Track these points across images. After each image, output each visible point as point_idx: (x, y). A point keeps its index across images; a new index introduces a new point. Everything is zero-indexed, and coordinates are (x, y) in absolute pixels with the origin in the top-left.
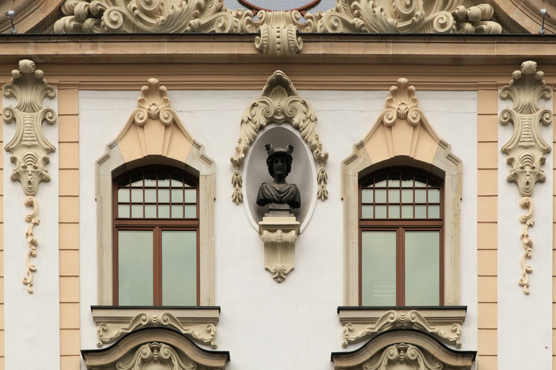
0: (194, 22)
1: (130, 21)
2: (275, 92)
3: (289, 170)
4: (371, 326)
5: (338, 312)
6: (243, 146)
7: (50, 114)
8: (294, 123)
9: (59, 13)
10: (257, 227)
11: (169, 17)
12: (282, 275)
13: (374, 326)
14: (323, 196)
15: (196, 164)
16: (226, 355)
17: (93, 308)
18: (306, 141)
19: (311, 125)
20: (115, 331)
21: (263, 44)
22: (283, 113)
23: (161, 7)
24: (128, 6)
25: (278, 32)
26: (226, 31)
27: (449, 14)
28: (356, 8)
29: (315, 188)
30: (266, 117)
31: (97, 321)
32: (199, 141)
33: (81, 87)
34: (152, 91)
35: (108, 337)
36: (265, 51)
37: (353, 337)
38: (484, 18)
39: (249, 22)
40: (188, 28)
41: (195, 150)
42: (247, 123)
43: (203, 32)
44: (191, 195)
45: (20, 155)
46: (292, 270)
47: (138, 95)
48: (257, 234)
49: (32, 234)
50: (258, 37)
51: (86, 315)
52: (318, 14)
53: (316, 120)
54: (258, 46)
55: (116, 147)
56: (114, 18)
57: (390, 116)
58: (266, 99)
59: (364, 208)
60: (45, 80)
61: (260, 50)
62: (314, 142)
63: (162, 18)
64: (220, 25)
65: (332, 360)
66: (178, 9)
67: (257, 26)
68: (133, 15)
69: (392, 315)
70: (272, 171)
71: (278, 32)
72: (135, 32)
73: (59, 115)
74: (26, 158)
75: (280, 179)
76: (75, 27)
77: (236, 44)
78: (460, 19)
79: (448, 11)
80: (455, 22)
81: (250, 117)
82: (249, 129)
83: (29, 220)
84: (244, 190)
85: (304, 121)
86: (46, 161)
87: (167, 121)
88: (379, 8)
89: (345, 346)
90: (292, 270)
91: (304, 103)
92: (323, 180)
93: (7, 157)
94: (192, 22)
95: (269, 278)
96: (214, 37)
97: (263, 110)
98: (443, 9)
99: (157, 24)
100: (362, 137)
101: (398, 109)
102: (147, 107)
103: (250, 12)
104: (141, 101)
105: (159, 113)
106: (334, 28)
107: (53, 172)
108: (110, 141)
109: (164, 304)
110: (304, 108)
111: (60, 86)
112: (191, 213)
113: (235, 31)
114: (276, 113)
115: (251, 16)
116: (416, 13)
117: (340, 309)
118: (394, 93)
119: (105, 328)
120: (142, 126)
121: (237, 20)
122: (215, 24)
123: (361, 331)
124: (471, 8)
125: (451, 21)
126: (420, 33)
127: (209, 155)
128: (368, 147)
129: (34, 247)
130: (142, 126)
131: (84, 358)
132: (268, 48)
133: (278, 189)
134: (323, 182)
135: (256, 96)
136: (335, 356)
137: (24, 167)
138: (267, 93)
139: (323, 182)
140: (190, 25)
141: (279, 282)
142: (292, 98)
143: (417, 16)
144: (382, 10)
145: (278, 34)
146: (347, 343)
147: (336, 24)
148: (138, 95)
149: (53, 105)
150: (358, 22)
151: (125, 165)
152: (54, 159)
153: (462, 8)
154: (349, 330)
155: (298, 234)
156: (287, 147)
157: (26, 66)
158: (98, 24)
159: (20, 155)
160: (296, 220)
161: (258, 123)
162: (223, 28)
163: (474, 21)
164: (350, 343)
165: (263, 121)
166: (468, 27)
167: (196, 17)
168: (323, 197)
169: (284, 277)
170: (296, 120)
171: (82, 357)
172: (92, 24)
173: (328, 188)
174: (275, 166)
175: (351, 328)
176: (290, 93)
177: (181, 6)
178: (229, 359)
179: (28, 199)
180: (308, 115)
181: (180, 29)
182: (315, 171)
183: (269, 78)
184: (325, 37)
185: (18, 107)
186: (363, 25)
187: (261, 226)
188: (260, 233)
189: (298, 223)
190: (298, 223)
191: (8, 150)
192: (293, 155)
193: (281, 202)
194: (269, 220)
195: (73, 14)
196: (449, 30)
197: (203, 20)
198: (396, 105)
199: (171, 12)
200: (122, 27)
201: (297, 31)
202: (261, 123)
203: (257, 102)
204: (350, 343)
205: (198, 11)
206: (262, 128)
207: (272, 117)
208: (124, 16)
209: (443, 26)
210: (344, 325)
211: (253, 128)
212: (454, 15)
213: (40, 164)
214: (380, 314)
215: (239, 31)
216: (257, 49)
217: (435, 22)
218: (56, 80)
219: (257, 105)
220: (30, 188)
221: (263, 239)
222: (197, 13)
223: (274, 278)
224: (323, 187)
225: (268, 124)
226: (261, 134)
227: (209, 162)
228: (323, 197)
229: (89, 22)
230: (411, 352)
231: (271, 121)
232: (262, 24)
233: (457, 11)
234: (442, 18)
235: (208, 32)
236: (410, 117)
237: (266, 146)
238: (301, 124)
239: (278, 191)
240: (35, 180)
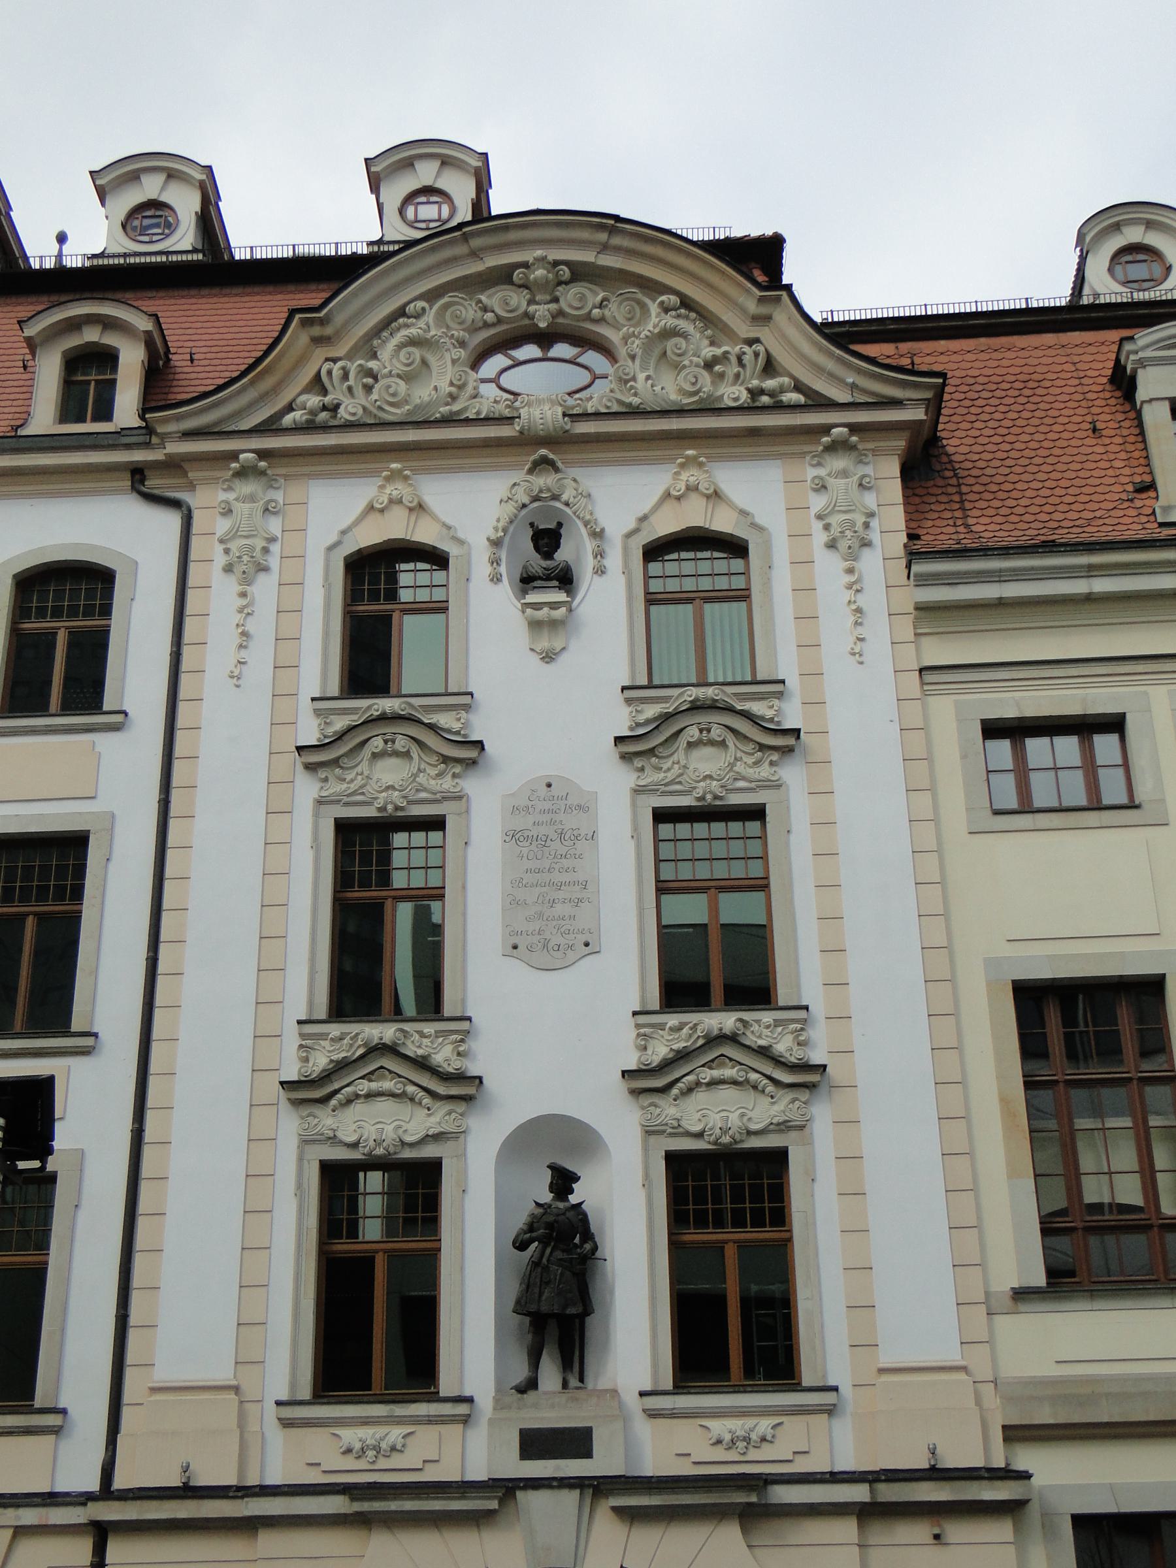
0: (444, 409)
1: (371, 412)
2: (540, 470)
3: (558, 546)
4: (664, 705)
5: (622, 692)
6: (500, 525)
7: (273, 504)
8: (563, 500)
9: (290, 408)
10: (519, 606)
11: (416, 406)
12: (551, 655)
13: (668, 705)
14: (600, 571)
15: (444, 546)
16: (479, 745)
17: (313, 699)
18: (578, 517)
19: (584, 500)
20: (340, 723)
21: (523, 426)
22: (549, 490)
23: (408, 399)
24: (369, 399)
25: (542, 414)
26: (482, 417)
27: (742, 389)
28: (632, 387)
29: (589, 562)
30: (529, 495)
31: (318, 713)
32: (449, 521)
33: (311, 476)
34: (393, 476)
35: (330, 731)
36: (526, 432)
37: (641, 718)
38: (782, 390)
39: (508, 406)
40: (438, 415)
41: (444, 531)
42: (506, 502)
43: (455, 418)
44: (439, 577)
45: (234, 546)
46: (564, 649)
47: (379, 482)
48: (521, 613)
49: (243, 625)
50: (517, 420)
51: (305, 705)
52: (589, 396)
53: (589, 495)
54: (518, 428)
55: (351, 533)
56: (353, 410)
57: (677, 488)
58: (529, 478)
59: (652, 581)
60: (269, 472)
61: (521, 432)
62: (588, 517)
63: (407, 407)
64: (474, 411)
65: (616, 745)
66: (426, 399)
67: (517, 409)
68: (374, 407)
70: (537, 549)
71: (542, 414)
72: (377, 422)
73: (284, 505)
74: (240, 549)
75: (548, 555)
76: (307, 421)
77: (493, 427)
78: (755, 393)
79: (740, 385)
80: (749, 396)
81: (510, 496)
82: (510, 508)
83: (240, 611)
84: (503, 569)
85: (574, 497)
86: (266, 550)
87: (410, 505)
88: (660, 387)
89: (631, 729)
90: (564, 649)
91: (575, 480)
92: (599, 554)
93: (219, 548)
94: (441, 409)
95: (535, 659)
96: (468, 421)
97: (525, 490)
98: (734, 384)
99: (402, 414)
100: (646, 508)
101: (687, 481)
102: (388, 491)
103: (511, 397)
104: (382, 487)
105: (402, 497)
106: (608, 407)
107: (274, 562)
108: (344, 525)
109: (403, 692)
110: (574, 484)
111: (286, 477)
112: (439, 594)
113: (491, 415)
114: (541, 491)
115: (510, 400)
116: (704, 390)
117: (624, 689)
118: (682, 466)
119: (328, 721)
120: (382, 511)
121: (495, 405)
122: (469, 410)
123: (651, 711)
124: (767, 382)
125: (744, 396)
126: (709, 407)
127: (461, 535)
128: (653, 519)
129: (245, 638)
130: (382, 511)
131: (299, 755)
132: (529, 429)
133: (545, 566)
134: (599, 556)
135: (519, 476)
136: (619, 740)
137: (239, 557)
138: (531, 471)
139: (599, 556)
140: (439, 412)
141: (547, 663)
142: (559, 476)
143: (704, 392)
144: (662, 389)
145: (541, 416)
146: (634, 725)
147: (609, 404)
148: (379, 482)
149: (278, 496)
150: (635, 401)
151: (360, 551)
152: (275, 548)
153: (755, 383)
154: (636, 710)
155: (570, 610)
156: (555, 524)
157: (247, 460)
158: (335, 417)
159: (234, 546)
160: (567, 597)
161: (519, 501)
162: (478, 413)
163: (771, 394)
164: (638, 725)
165: (526, 500)
166: (765, 399)
167: (447, 404)
168: (599, 572)
169: (554, 657)
170: (565, 497)
171: (297, 754)
172: (328, 417)
173: (607, 562)
174: (541, 542)
175: (639, 709)
176: (557, 470)
177: (430, 395)
178: (483, 749)
179: (240, 588)
180: (580, 491)
181: (428, 417)
182: (589, 545)
183: (532, 458)
184: (597, 415)
185: (236, 499)
186: (641, 403)
187: (522, 604)
188: (523, 612)
189: (569, 599)
190: (569, 599)
191: (221, 541)
192: (562, 531)
193: (548, 578)
194: (532, 598)
195: (305, 409)
196: (743, 403)
197: (456, 407)
198: (684, 476)
199: (418, 401)
200: (361, 417)
201: (564, 412)
202: (523, 501)
203: (518, 481)
204: (638, 725)
205: (449, 399)
206: (524, 506)
207: (537, 495)
208: (364, 409)
209: (736, 399)
210: (629, 705)
211: (514, 507)
212: (749, 390)
213: (258, 553)
214: (675, 692)
215: (497, 416)
216: (518, 431)
217: (725, 397)
218: (283, 471)
219: (519, 484)
220: (245, 578)
221: (526, 618)
222: (448, 402)
223: (541, 659)
224: (599, 561)
225: (531, 503)
226: (524, 512)
227: (461, 542)
228: (599, 572)
229: (324, 415)
231: (536, 499)
232: (522, 408)
233: (750, 386)
234: (734, 393)
235: (463, 417)
236: (700, 487)
237: (530, 524)
238: (571, 500)
239: (544, 568)
240: (251, 569)
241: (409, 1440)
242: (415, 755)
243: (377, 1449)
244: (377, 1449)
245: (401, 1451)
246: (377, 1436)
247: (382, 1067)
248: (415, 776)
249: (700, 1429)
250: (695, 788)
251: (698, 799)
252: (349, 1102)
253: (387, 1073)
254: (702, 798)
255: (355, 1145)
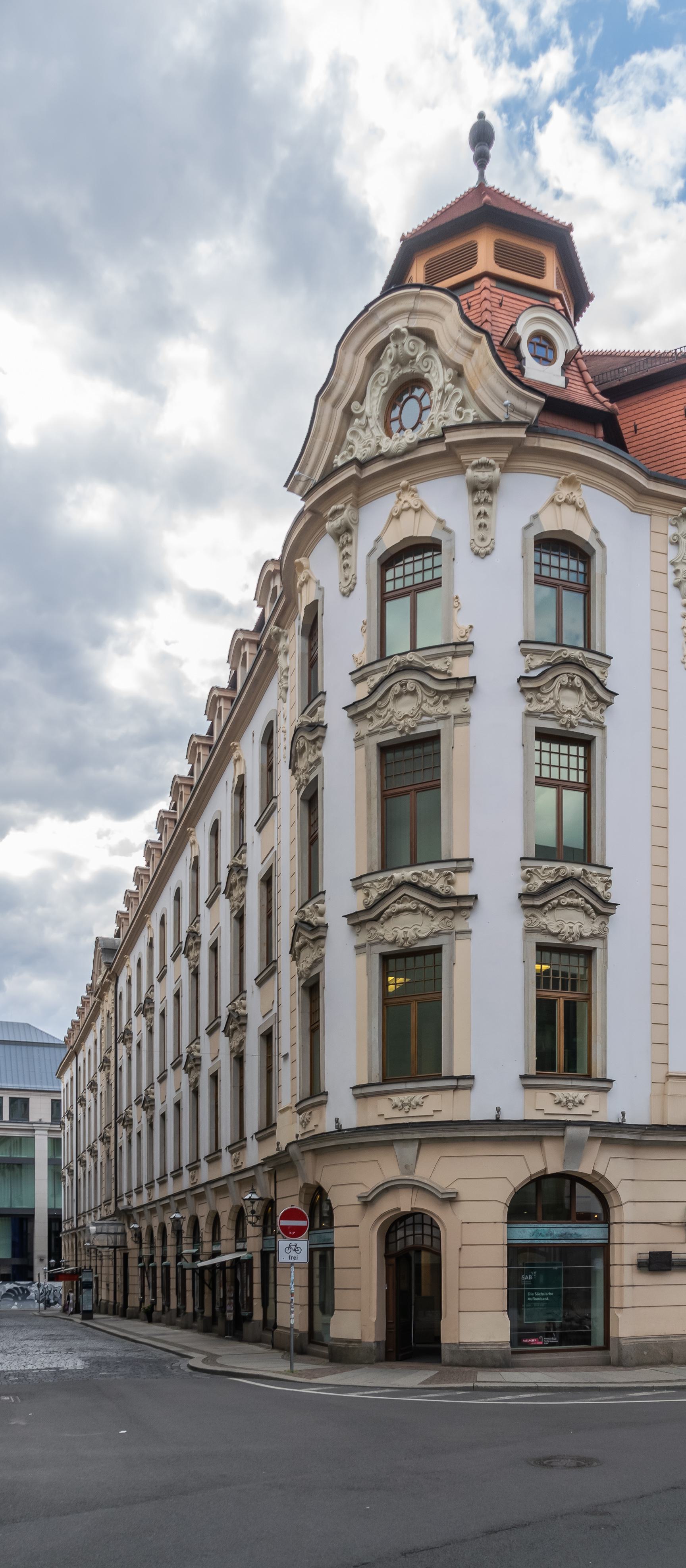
69: (565, 652)
230: (577, 680)
241: (425, 1100)
242: (419, 692)
243: (409, 1105)
244: (409, 1105)
245: (422, 1106)
246: (409, 1099)
247: (405, 895)
248: (420, 706)
249: (550, 1096)
250: (561, 717)
251: (562, 725)
252: (389, 917)
253: (408, 898)
254: (565, 726)
255: (394, 942)
